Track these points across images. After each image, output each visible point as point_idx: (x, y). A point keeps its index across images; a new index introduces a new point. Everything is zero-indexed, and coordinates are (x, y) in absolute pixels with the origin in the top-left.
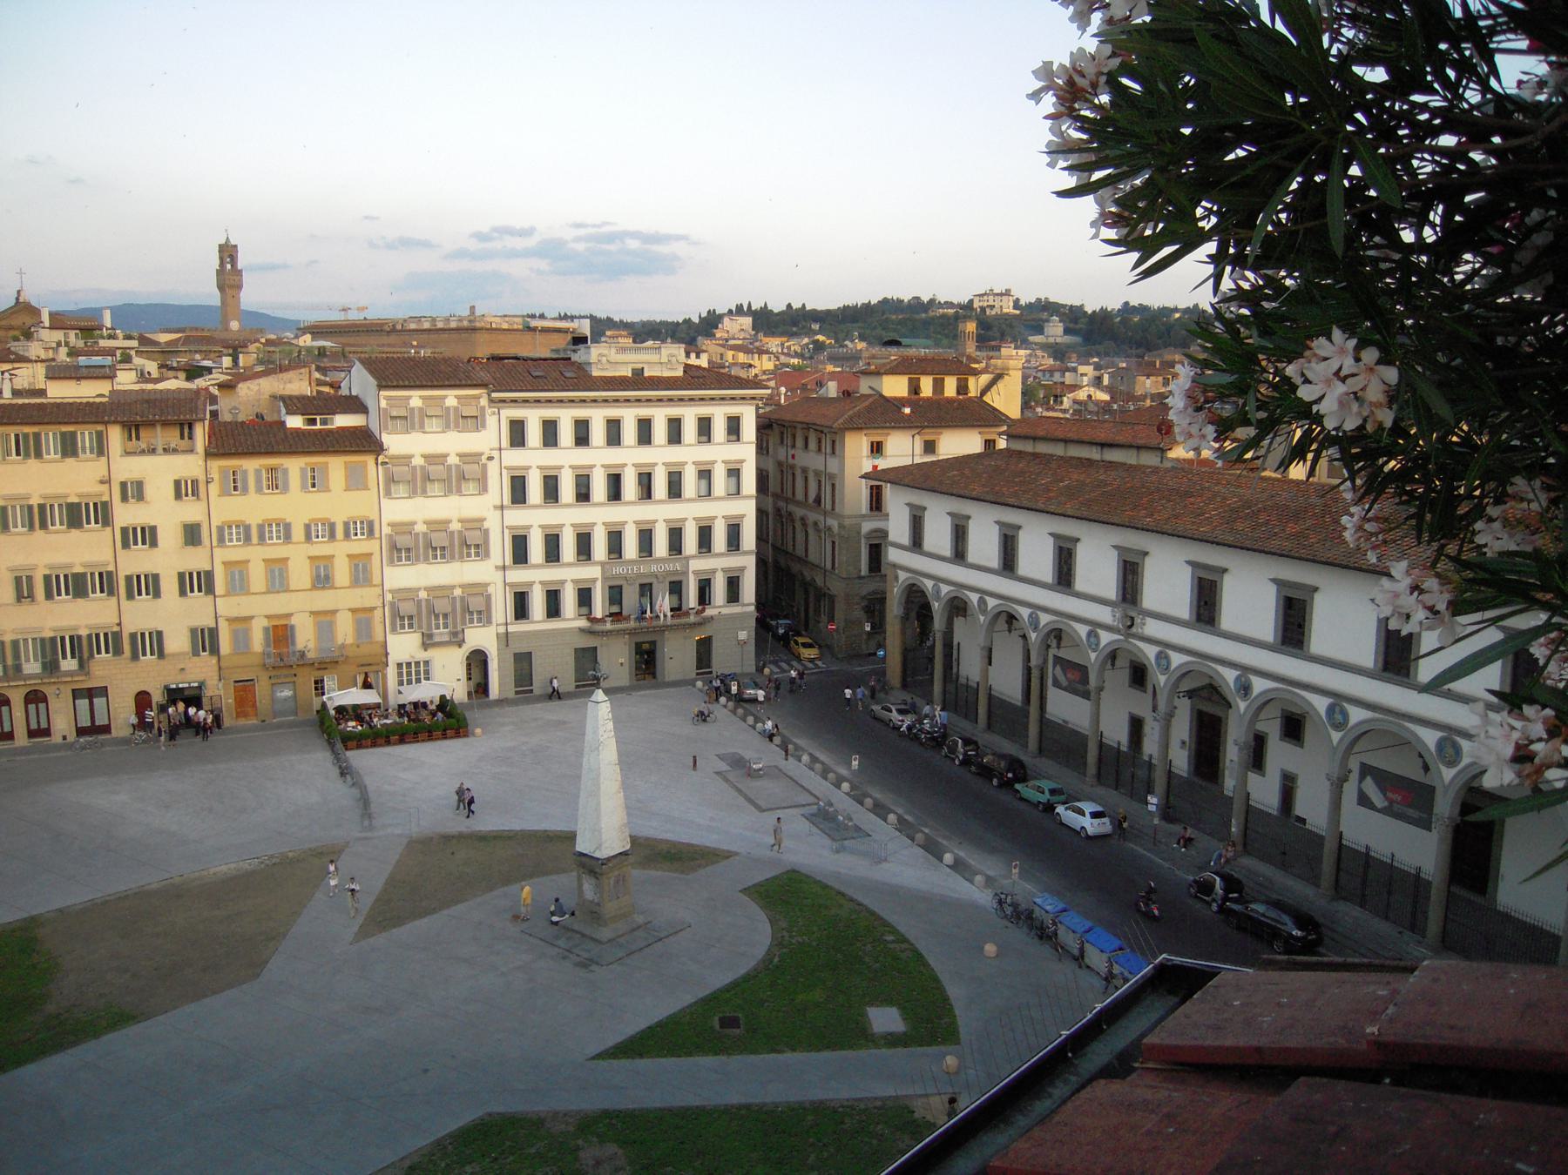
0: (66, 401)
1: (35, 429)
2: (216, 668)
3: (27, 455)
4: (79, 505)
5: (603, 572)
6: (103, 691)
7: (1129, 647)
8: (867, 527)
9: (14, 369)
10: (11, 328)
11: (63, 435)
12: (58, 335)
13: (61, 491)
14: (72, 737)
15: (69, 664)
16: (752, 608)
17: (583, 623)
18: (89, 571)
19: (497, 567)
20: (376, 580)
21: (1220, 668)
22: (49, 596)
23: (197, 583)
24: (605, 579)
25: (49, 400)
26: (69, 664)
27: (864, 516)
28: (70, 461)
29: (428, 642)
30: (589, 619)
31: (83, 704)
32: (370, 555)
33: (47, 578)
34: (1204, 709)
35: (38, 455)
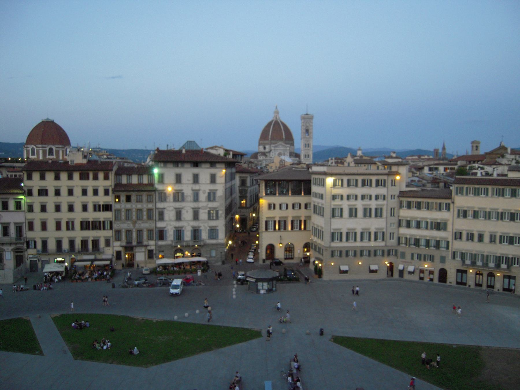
0: (514, 178)
1: (503, 187)
3: (499, 196)
4: (514, 213)
6: (514, 278)
9: (497, 167)
10: (497, 154)
11: (512, 189)
12: (513, 156)
13: (509, 208)
14: (501, 291)
15: (504, 266)
18: (515, 236)
22: (500, 242)
25: (509, 178)
26: (504, 266)
28: (514, 199)
31: (507, 280)
33: (501, 237)
35: (503, 196)
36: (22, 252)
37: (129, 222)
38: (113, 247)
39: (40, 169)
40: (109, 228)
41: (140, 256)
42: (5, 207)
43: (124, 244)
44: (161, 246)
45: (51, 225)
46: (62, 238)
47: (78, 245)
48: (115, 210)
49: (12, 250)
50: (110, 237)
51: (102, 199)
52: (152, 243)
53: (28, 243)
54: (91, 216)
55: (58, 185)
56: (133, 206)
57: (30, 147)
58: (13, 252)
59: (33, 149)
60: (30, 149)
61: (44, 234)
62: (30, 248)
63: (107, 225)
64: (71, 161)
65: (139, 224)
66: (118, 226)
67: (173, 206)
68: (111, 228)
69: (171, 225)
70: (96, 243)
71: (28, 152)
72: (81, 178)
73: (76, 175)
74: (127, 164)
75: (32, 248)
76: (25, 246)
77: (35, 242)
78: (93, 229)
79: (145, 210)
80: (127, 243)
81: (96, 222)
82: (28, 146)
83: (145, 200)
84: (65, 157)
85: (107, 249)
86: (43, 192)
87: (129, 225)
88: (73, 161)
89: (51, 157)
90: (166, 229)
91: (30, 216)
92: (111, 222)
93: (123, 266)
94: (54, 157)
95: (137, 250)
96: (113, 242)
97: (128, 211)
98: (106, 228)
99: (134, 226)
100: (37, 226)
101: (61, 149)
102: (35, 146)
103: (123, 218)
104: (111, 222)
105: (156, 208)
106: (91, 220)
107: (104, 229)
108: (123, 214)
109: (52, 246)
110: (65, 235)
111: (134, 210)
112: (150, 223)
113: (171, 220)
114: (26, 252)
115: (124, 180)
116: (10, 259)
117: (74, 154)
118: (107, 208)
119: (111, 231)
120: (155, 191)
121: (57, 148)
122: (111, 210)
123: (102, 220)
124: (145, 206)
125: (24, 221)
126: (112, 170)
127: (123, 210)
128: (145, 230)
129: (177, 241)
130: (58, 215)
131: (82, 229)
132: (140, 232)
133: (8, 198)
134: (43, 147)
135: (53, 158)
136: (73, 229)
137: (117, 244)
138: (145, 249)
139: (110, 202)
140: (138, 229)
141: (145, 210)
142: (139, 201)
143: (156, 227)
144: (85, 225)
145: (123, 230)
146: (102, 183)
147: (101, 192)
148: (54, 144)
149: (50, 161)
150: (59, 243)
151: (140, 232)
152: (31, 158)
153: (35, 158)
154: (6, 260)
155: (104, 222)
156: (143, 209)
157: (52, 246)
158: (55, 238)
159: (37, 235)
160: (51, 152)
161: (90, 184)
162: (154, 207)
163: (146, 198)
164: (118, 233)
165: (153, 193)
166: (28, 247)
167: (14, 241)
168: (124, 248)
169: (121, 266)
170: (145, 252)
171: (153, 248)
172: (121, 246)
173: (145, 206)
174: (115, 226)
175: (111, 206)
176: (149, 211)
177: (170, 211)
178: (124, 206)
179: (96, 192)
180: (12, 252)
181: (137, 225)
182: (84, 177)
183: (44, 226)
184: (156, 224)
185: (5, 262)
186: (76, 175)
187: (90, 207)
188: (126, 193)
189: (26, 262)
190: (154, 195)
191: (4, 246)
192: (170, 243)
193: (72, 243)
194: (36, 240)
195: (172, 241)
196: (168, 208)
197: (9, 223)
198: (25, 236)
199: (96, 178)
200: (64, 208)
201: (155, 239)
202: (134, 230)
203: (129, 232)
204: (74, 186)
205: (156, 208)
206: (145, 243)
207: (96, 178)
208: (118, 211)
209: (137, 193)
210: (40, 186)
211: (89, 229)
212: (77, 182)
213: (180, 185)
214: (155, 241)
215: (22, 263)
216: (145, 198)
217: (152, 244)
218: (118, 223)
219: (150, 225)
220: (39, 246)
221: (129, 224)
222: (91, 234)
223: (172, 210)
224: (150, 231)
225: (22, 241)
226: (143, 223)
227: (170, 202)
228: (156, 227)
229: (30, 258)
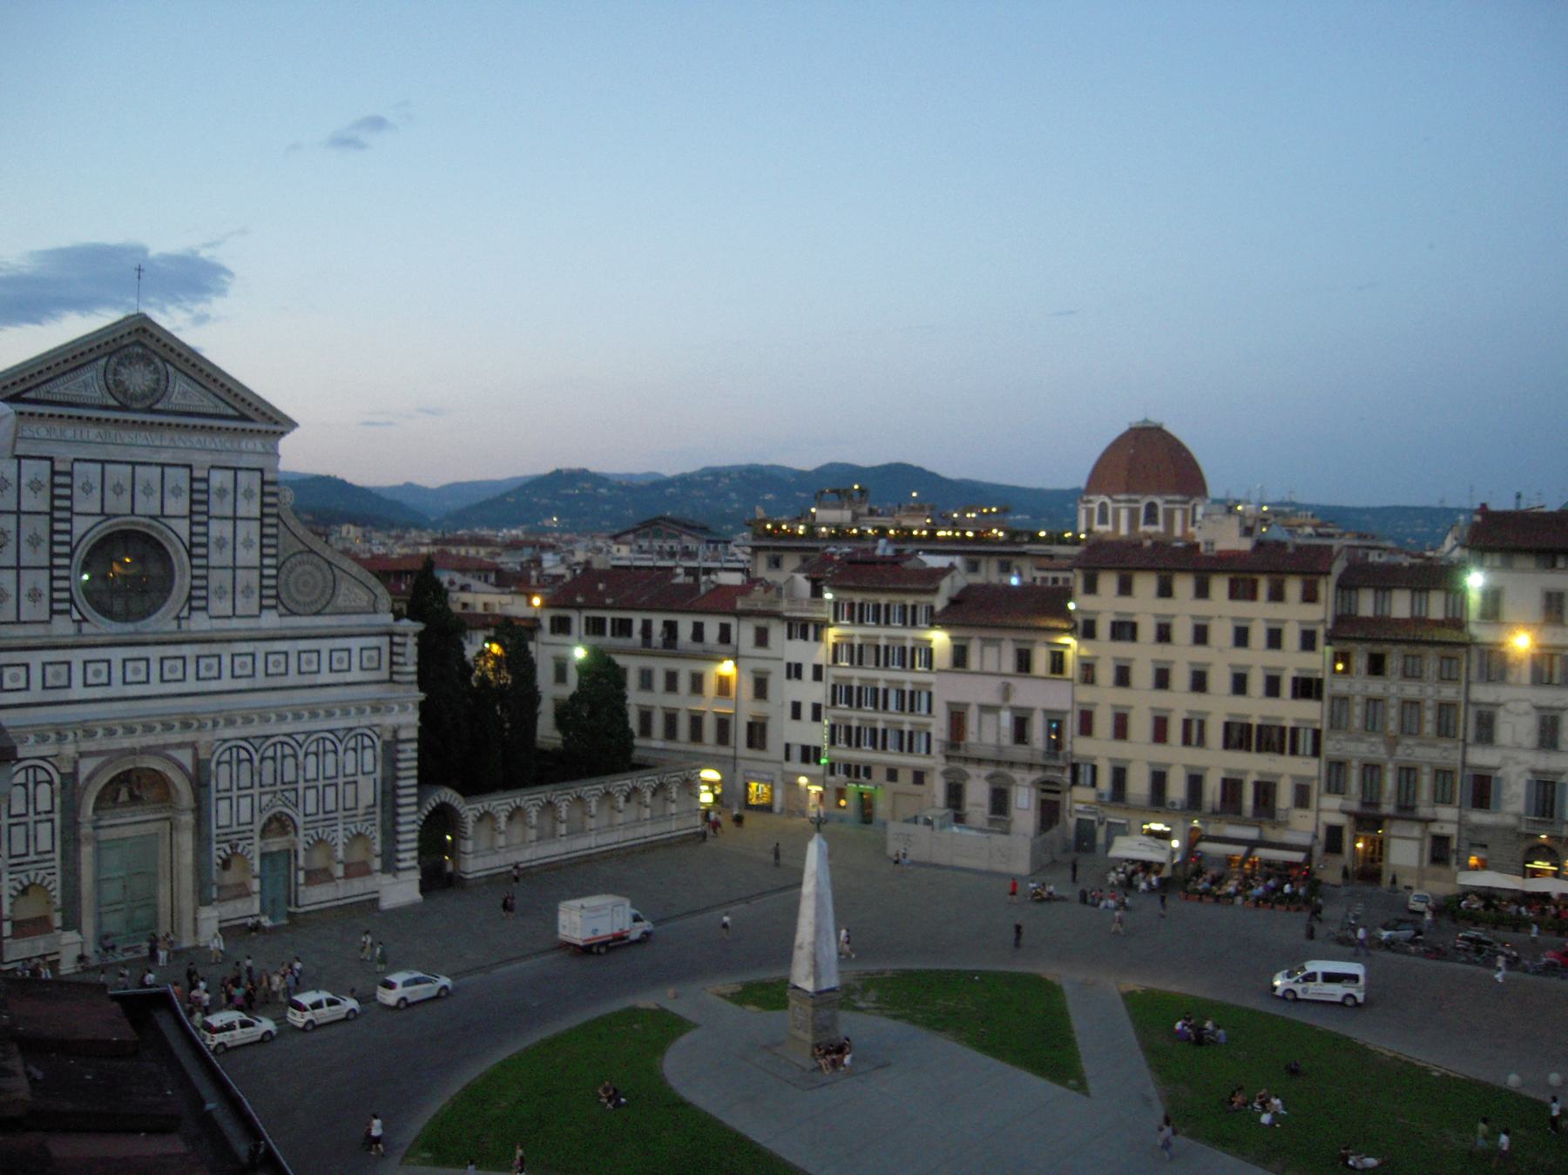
36: (1058, 792)
37: (1373, 740)
38: (1319, 810)
39: (1122, 565)
40: (1309, 751)
41: (1404, 852)
42: (1024, 663)
43: (1354, 806)
44: (1479, 828)
45: (1141, 726)
46: (1169, 765)
47: (1212, 792)
48: (1333, 698)
49: (1034, 783)
50: (1312, 779)
51: (1293, 661)
52: (1448, 813)
53: (1075, 768)
54: (1256, 708)
55: (1168, 611)
56: (1392, 687)
57: (1097, 500)
58: (1037, 788)
59: (1103, 506)
60: (1096, 506)
61: (1121, 750)
62: (1080, 785)
63: (1305, 741)
64: (1207, 543)
65: (1409, 747)
66: (1338, 746)
67: (1528, 700)
68: (1316, 752)
69: (1518, 763)
70: (1265, 791)
71: (1090, 512)
72: (1234, 595)
73: (1219, 586)
74: (1377, 552)
75: (1085, 785)
76: (1067, 777)
77: (1094, 769)
78: (1259, 750)
79: (1430, 703)
80: (1364, 804)
81: (1270, 727)
82: (1091, 498)
83: (1430, 673)
84: (1191, 529)
85: (1299, 812)
86: (1124, 630)
87: (1373, 748)
88: (1212, 544)
89: (1151, 529)
90: (1500, 773)
91: (1085, 694)
92: (1317, 734)
93: (1345, 874)
94: (1160, 528)
95: (1393, 831)
96: (1319, 795)
97: (1373, 702)
98: (1301, 750)
99: (1392, 753)
100: (1104, 723)
101: (1122, 505)
102: (1110, 498)
103: (1357, 723)
104: (1317, 734)
105: (1468, 701)
106: (1255, 721)
107: (1294, 751)
108: (1358, 711)
109: (1138, 785)
110: (1178, 758)
111: (1393, 701)
112: (1446, 749)
113: (1519, 747)
114: (1068, 795)
115: (1366, 605)
116: (1025, 806)
117: (1214, 522)
118: (1307, 688)
119: (1315, 761)
120: (1466, 645)
121: (1167, 502)
122: (1319, 697)
123: (1288, 723)
124: (1431, 692)
125: (1067, 706)
126: (1328, 573)
127: (1358, 699)
128: (1426, 769)
129: (1537, 819)
130: (1162, 699)
131: (1227, 745)
132: (1408, 774)
133: (1033, 642)
134: (1130, 501)
135: (1157, 533)
136: (1201, 742)
137: (1333, 802)
138: (1424, 831)
139: (1317, 671)
140: (1405, 765)
141: (1430, 703)
142: (1411, 673)
143: (1464, 764)
144: (1239, 736)
145: (1355, 763)
146: (1294, 613)
147: (1291, 638)
148: (1160, 493)
149: (1148, 543)
150: (1159, 780)
151: (1408, 774)
152: (1098, 532)
153: (1107, 532)
154: (1019, 809)
155: (1295, 731)
156: (1424, 700)
157: (1138, 785)
158: (1151, 764)
159: (1099, 749)
160: (1151, 517)
161: (1259, 612)
162: (1462, 699)
163: (1437, 665)
164: (1337, 768)
165: (1462, 650)
166: (1075, 781)
167: (1041, 761)
168: (1352, 819)
169: (1340, 873)
170: (1421, 840)
171: (1450, 830)
172: (1343, 812)
173: (1431, 692)
174: (1330, 747)
175: (1320, 682)
176: (1445, 708)
177: (1518, 714)
178: (1361, 685)
179: (1274, 639)
180: (1033, 791)
181: (1401, 753)
182: (1242, 591)
183: (1121, 728)
184: (1464, 753)
185: (1014, 813)
186: (1219, 586)
187: (1256, 684)
188: (1368, 646)
189: (1065, 821)
190: (1465, 655)
191: (1014, 770)
192: (1510, 821)
193: (1195, 782)
194: (1096, 763)
195: (1518, 816)
196: (1510, 706)
197: (1030, 710)
198: (1068, 748)
199: (1277, 595)
200: (1181, 678)
201: (1457, 803)
202: (1390, 766)
203: (1371, 770)
204: (1210, 618)
205: (1468, 701)
206: (1424, 811)
207: (1277, 595)
208: (1343, 700)
209: (1404, 647)
210: (1117, 613)
211: (1248, 749)
212: (1221, 607)
213: (1558, 630)
214: (1460, 807)
215: (1057, 822)
216: (1431, 664)
217: (1448, 819)
218: (1341, 737)
219: (1445, 754)
220: (1105, 782)
221: (1373, 744)
222: (1253, 765)
223: (1526, 713)
224: (1443, 775)
225: (1061, 763)
226: (1420, 745)
227: (1518, 685)
228: (1464, 764)
229: (1078, 811)
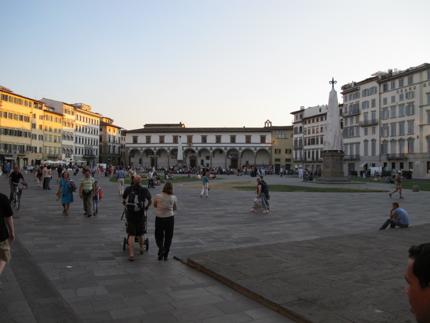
2: (42, 156)
5: (85, 146)
7: (190, 148)
8: (109, 144)
14: (23, 169)
16: (98, 157)
17: (82, 156)
19: (74, 143)
20: (61, 142)
21: (207, 148)
23: (41, 138)
24: (85, 147)
27: (108, 142)
29: (66, 157)
30: (83, 155)
32: (60, 137)
34: (246, 135)
